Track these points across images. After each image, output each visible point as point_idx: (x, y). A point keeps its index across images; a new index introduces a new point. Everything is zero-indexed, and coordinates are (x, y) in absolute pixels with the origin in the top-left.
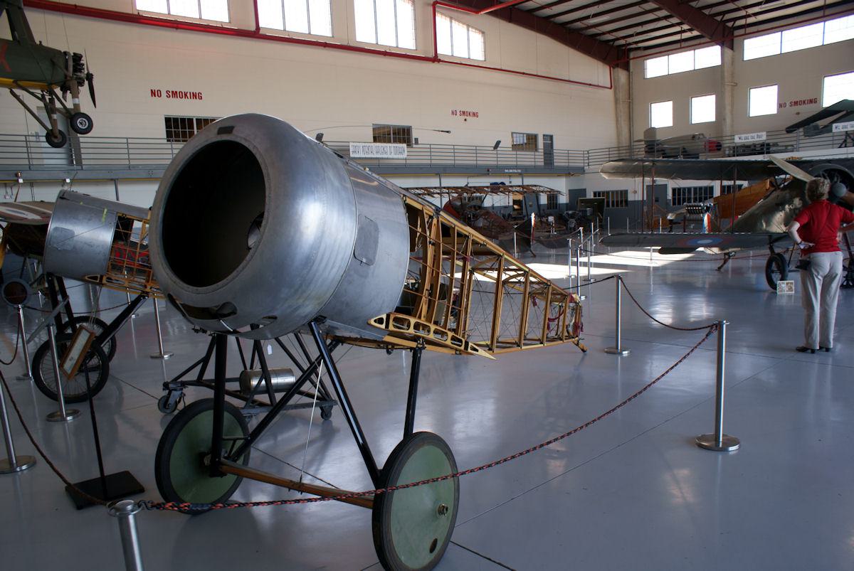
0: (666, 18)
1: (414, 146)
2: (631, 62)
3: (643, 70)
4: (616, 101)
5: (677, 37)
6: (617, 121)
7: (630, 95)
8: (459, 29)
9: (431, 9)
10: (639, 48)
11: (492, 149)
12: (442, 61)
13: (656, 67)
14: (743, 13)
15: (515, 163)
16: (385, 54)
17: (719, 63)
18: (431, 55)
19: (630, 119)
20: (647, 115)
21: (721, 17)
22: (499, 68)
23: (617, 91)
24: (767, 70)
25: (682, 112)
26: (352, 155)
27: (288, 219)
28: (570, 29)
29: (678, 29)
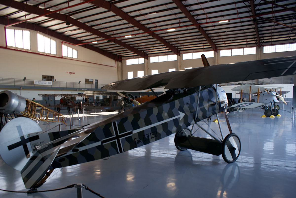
2: (122, 60)
3: (125, 62)
4: (118, 71)
6: (118, 76)
8: (70, 49)
10: (124, 57)
12: (64, 58)
13: (129, 62)
16: (46, 55)
17: (144, 63)
18: (61, 56)
20: (126, 75)
22: (81, 60)
24: (157, 65)
25: (135, 74)
26: (35, 84)
27: (11, 101)
28: (103, 50)
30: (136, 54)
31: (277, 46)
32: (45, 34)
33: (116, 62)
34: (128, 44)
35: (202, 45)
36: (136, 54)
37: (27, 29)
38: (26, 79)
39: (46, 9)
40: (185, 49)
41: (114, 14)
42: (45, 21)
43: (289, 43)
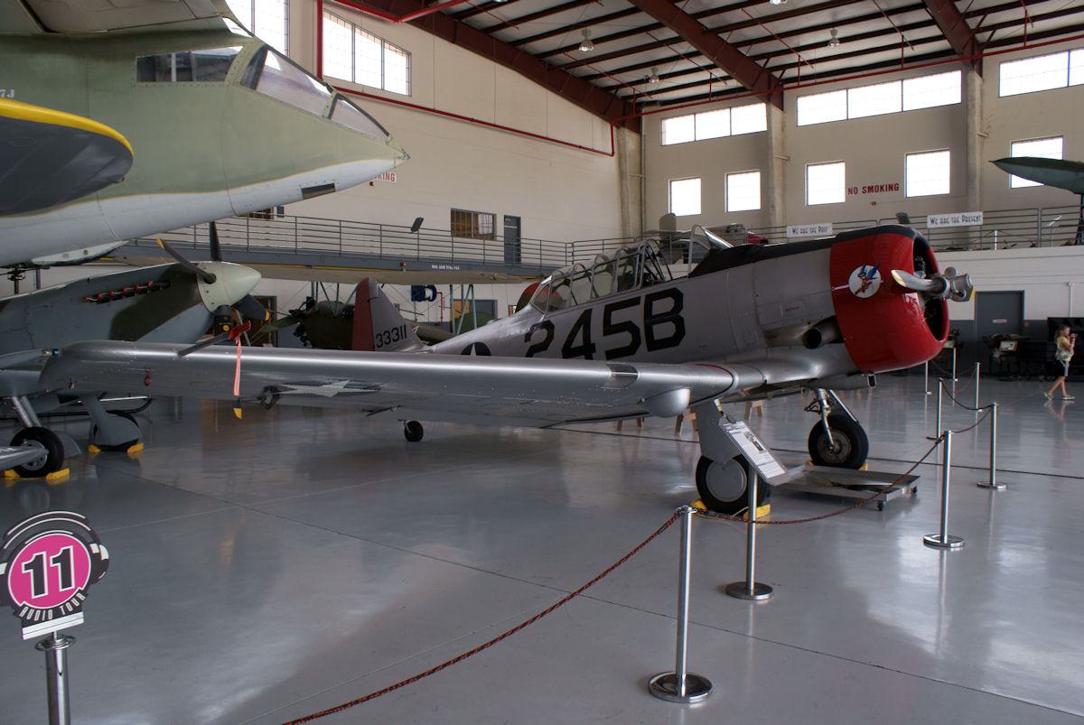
0: (689, 56)
1: (276, 218)
3: (659, 133)
4: (622, 174)
5: (704, 89)
6: (622, 203)
7: (641, 168)
8: (368, 46)
10: (654, 103)
11: (409, 230)
13: (677, 130)
14: (793, 58)
15: (450, 255)
19: (642, 203)
21: (781, 72)
23: (623, 160)
24: (834, 141)
25: (714, 194)
29: (705, 76)
33: (614, 128)
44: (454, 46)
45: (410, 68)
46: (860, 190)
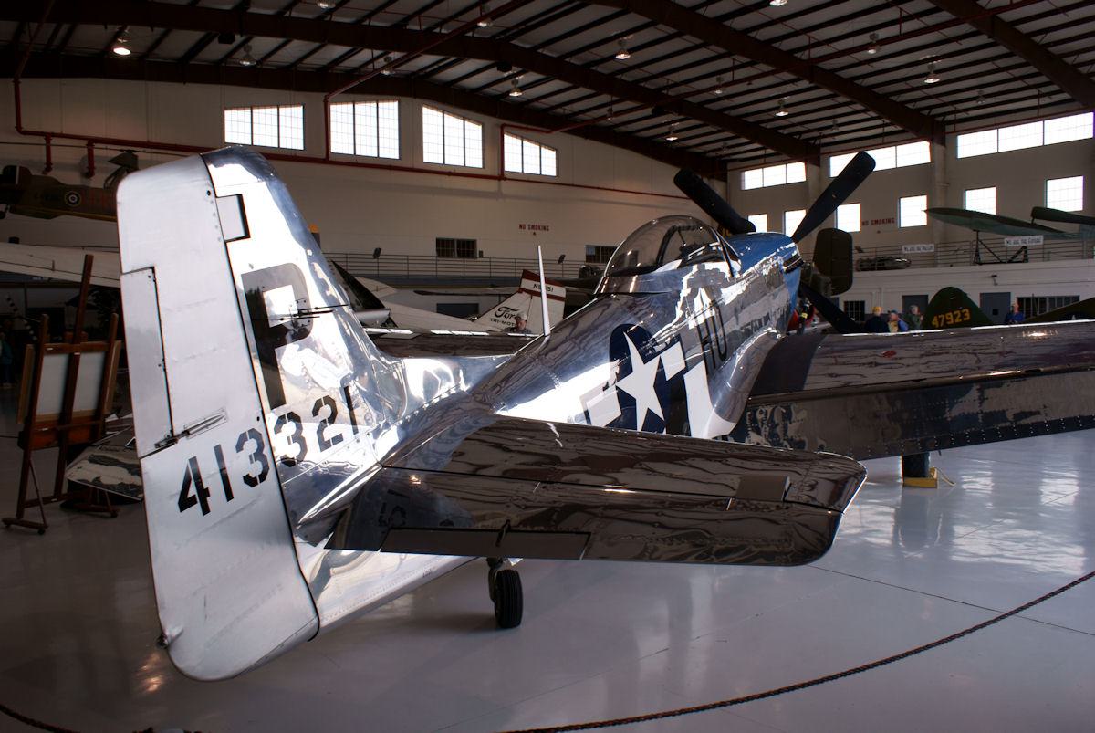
3: (740, 181)
8: (532, 149)
9: (500, 130)
13: (753, 179)
16: (449, 174)
17: (804, 179)
30: (769, 151)
31: (1046, 122)
32: (445, 107)
34: (734, 113)
35: (1034, 92)
36: (769, 151)
37: (389, 97)
38: (382, 252)
39: (429, 30)
40: (960, 116)
41: (642, 20)
42: (441, 64)
43: (1042, 118)
44: (588, 141)
45: (557, 159)
46: (870, 223)
